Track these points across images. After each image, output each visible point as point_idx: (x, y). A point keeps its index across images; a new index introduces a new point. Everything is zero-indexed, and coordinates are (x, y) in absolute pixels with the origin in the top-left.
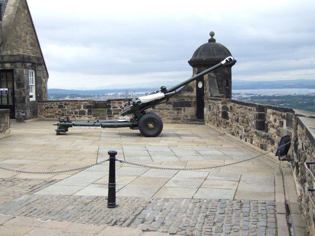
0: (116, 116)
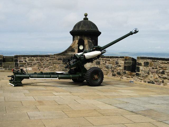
0: (21, 68)
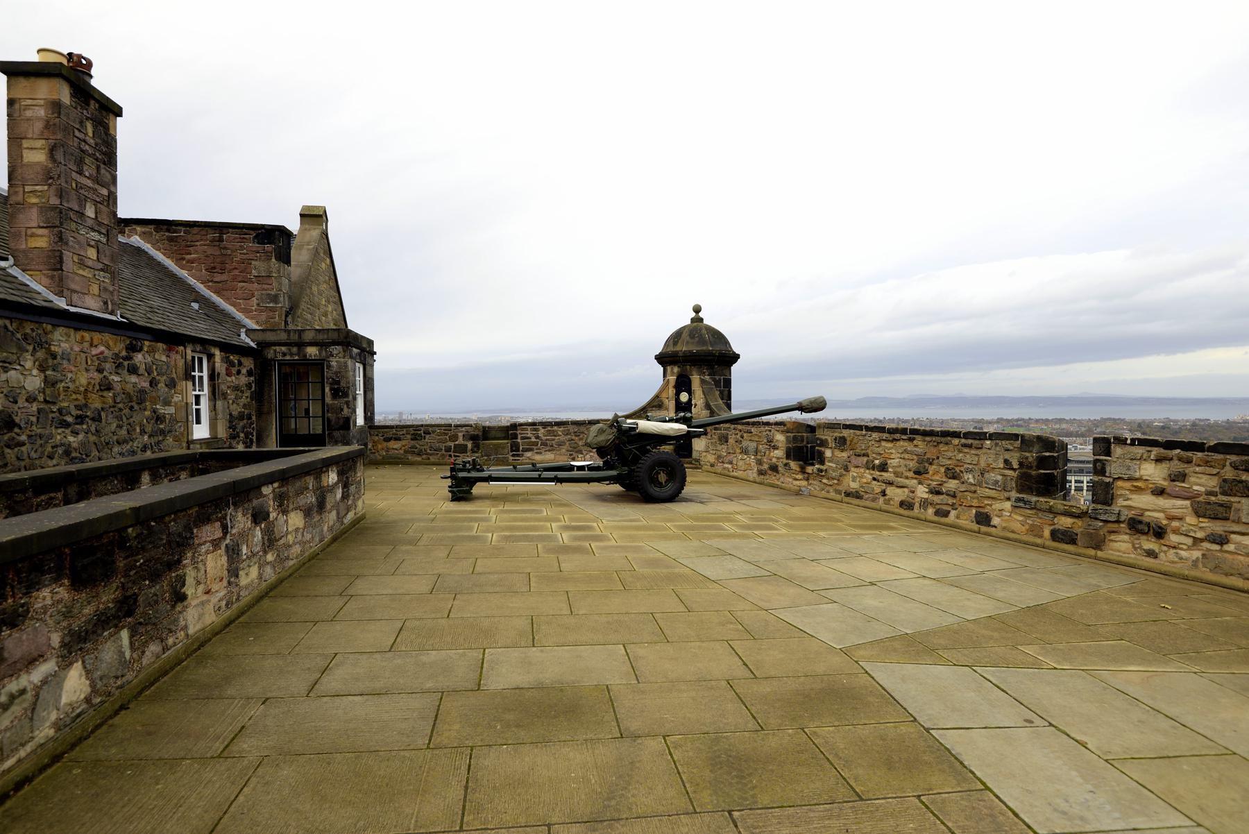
0: (529, 454)
